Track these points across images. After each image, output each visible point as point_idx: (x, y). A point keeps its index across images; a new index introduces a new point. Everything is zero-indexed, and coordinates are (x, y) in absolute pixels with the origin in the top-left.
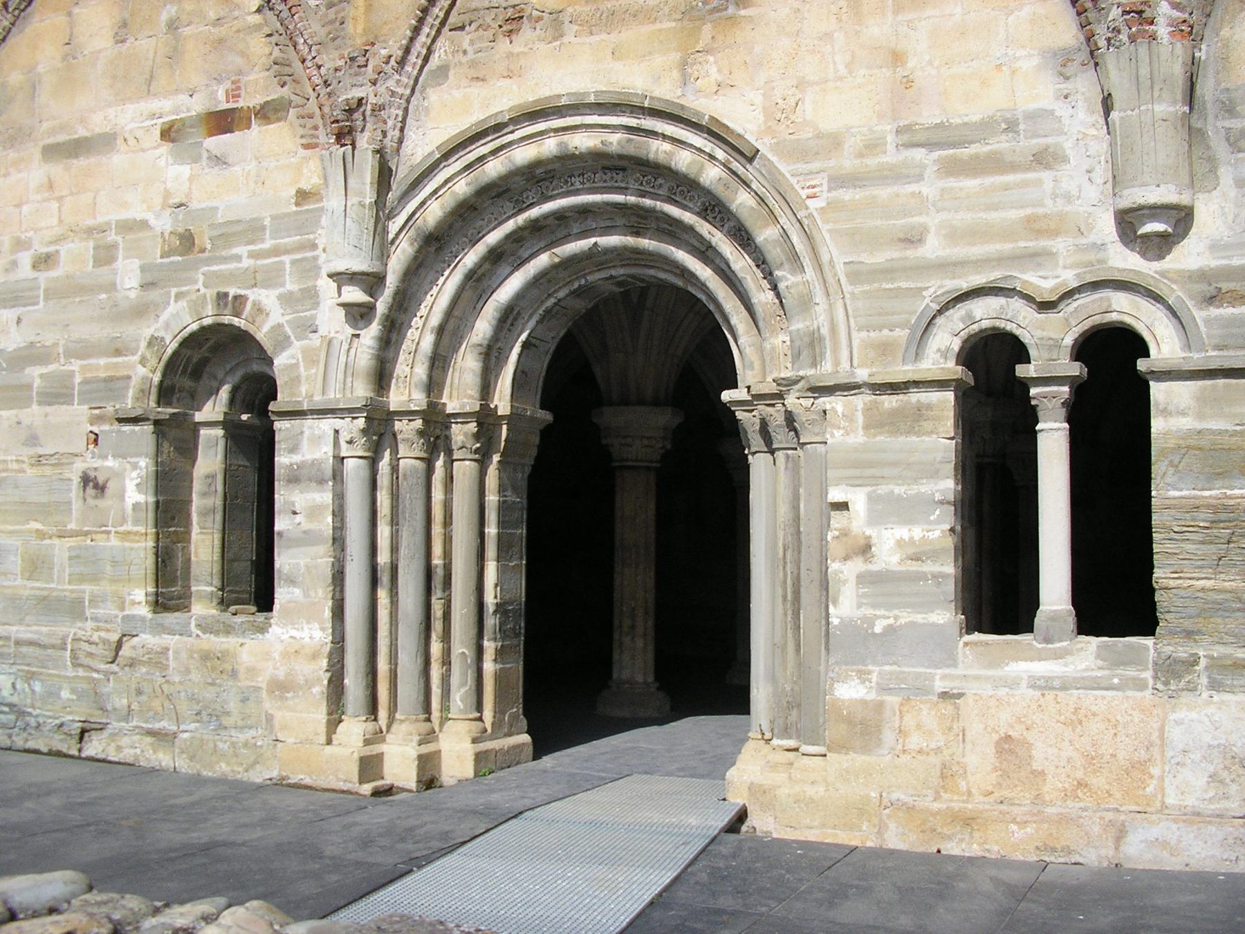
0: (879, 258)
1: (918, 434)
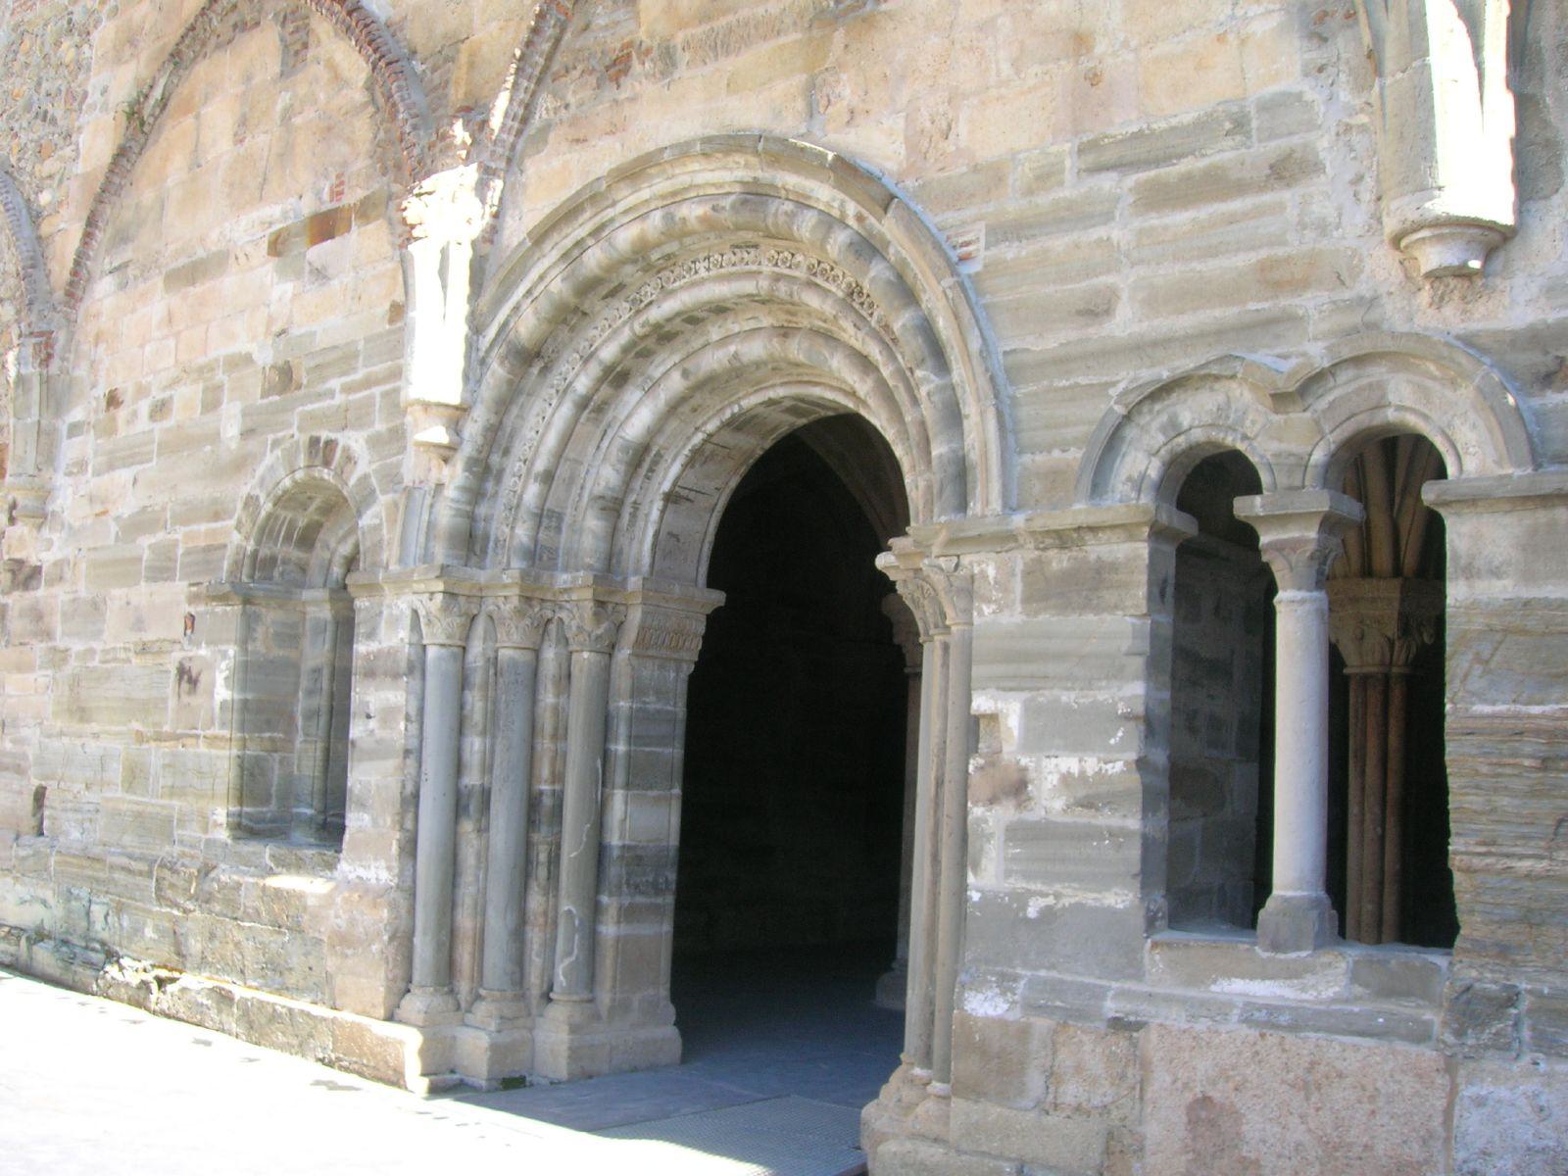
1: (1098, 610)
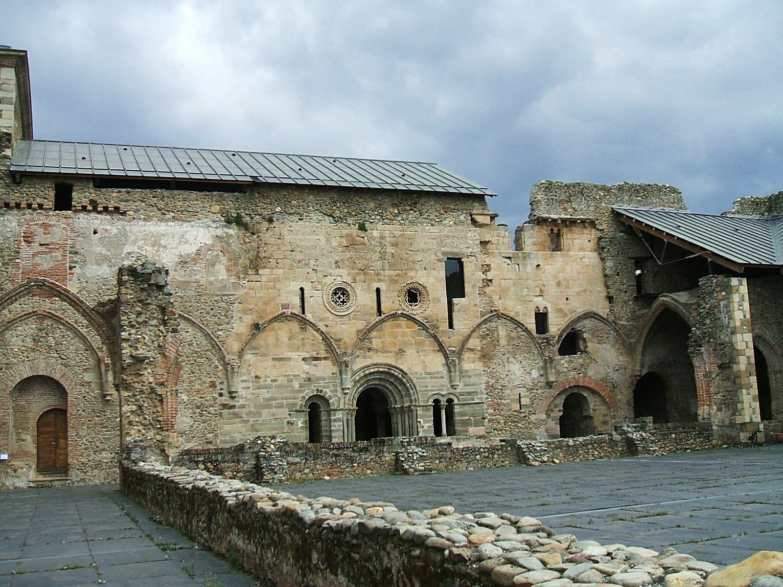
0: (422, 389)
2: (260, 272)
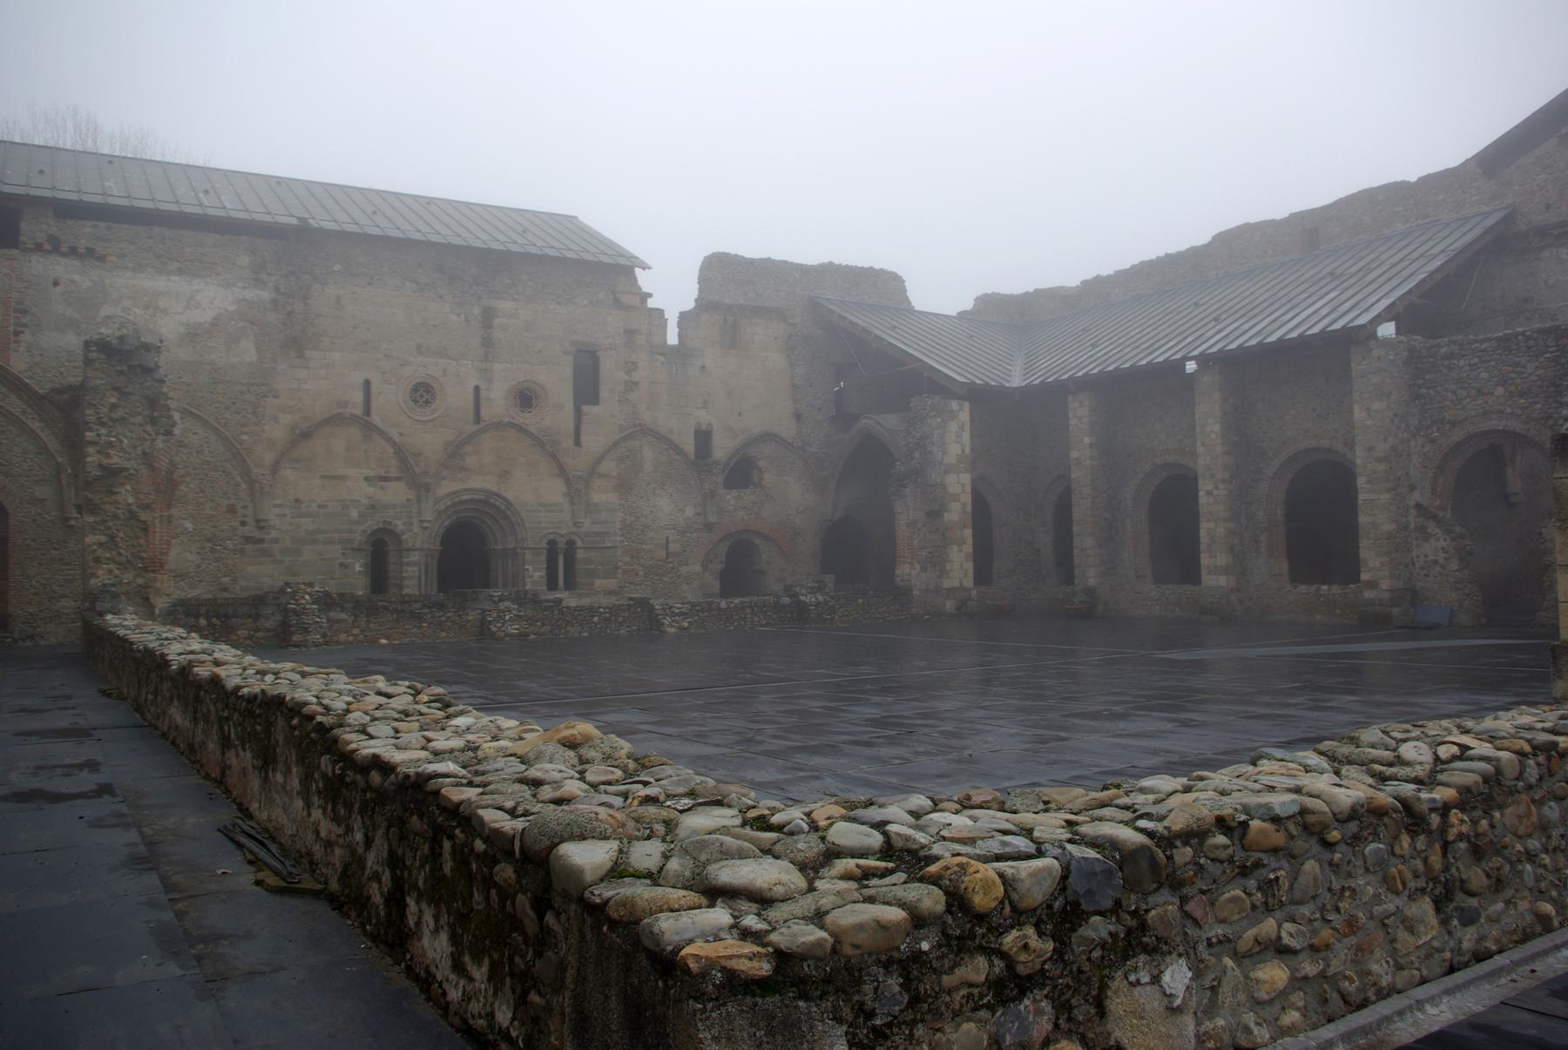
2: (308, 353)
